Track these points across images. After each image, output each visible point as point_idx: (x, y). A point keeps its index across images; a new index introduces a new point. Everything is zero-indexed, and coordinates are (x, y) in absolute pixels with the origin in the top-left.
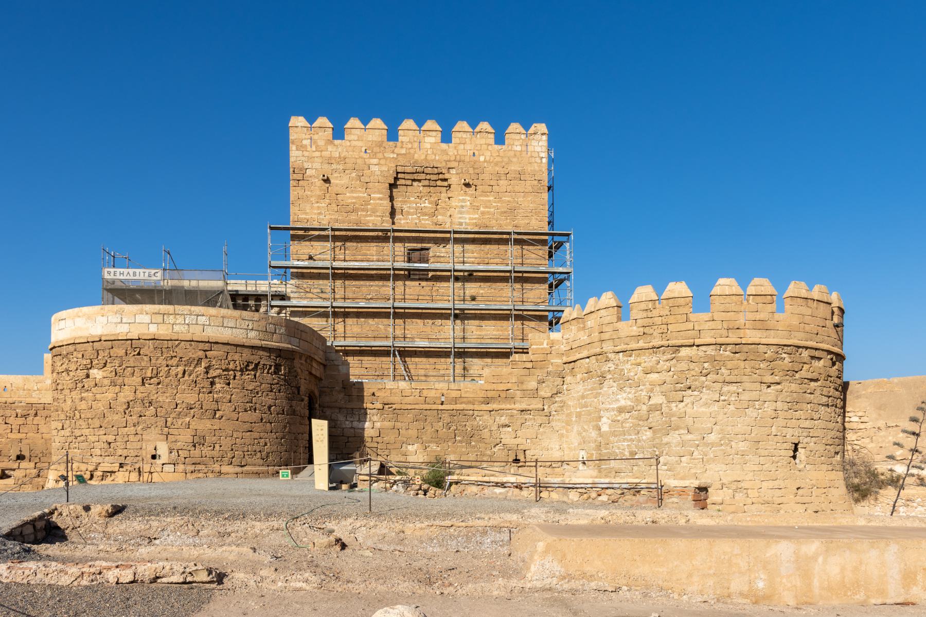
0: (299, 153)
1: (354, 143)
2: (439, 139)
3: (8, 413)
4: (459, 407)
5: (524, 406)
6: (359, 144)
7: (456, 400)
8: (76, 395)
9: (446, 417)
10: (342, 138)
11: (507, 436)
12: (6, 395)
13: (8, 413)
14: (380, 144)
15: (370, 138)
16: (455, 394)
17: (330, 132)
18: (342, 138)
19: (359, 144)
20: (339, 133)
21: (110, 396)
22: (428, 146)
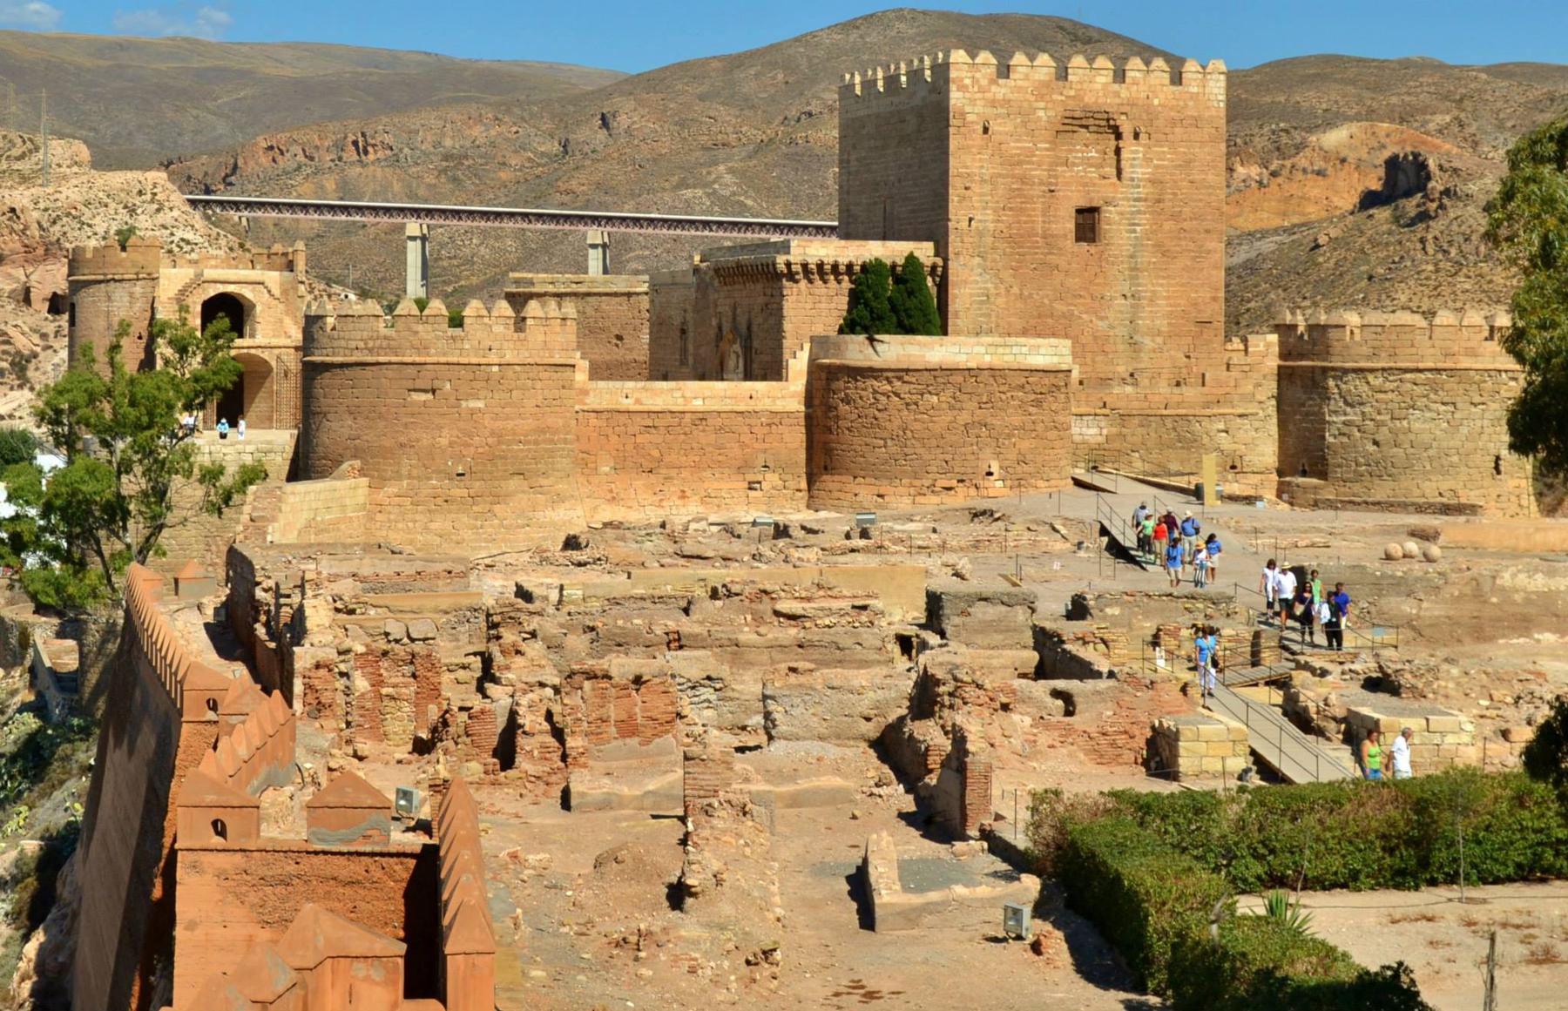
0: (960, 94)
1: (1020, 83)
2: (1110, 79)
3: (753, 421)
4: (1183, 412)
5: (1241, 411)
6: (1025, 84)
7: (1178, 405)
9: (1168, 422)
10: (1008, 77)
11: (1224, 441)
12: (752, 402)
13: (753, 421)
14: (1046, 84)
15: (1037, 77)
16: (1176, 398)
17: (993, 70)
18: (1008, 77)
19: (1025, 84)
20: (1004, 71)
22: (1099, 87)
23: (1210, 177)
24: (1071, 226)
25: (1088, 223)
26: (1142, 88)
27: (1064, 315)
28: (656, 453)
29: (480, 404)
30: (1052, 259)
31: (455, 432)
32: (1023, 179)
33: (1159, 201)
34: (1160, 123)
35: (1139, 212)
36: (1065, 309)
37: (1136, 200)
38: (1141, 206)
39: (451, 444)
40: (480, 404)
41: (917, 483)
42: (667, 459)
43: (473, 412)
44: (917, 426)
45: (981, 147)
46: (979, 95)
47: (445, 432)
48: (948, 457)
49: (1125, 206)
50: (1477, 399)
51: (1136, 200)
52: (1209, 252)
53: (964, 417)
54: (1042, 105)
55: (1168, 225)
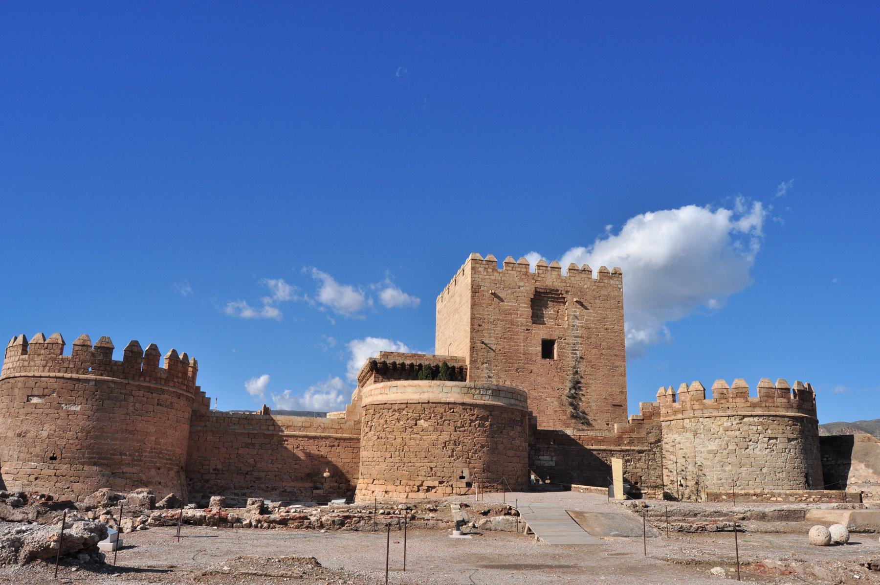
8: (406, 436)
21: (433, 437)
23: (616, 327)
24: (539, 348)
25: (547, 348)
26: (577, 278)
27: (536, 398)
28: (251, 461)
29: (78, 408)
30: (530, 367)
31: (53, 427)
32: (512, 322)
33: (588, 338)
34: (588, 297)
35: (577, 343)
36: (537, 395)
37: (576, 337)
38: (579, 340)
39: (48, 437)
40: (78, 408)
41: (411, 483)
42: (259, 465)
43: (68, 414)
44: (412, 442)
45: (488, 304)
46: (488, 277)
47: (46, 426)
48: (433, 465)
49: (571, 340)
50: (792, 436)
51: (576, 337)
52: (617, 367)
53: (445, 437)
54: (522, 284)
55: (594, 351)
